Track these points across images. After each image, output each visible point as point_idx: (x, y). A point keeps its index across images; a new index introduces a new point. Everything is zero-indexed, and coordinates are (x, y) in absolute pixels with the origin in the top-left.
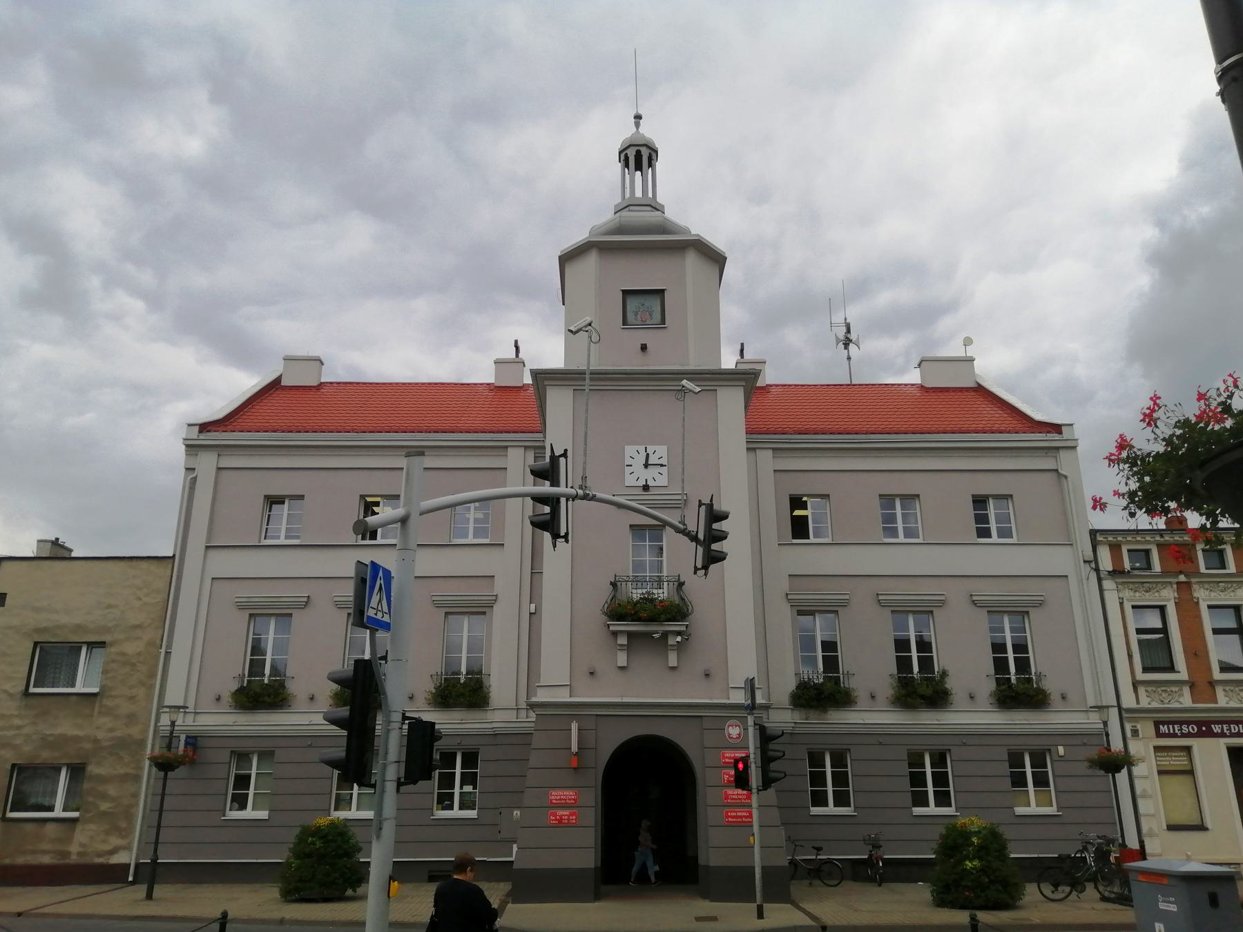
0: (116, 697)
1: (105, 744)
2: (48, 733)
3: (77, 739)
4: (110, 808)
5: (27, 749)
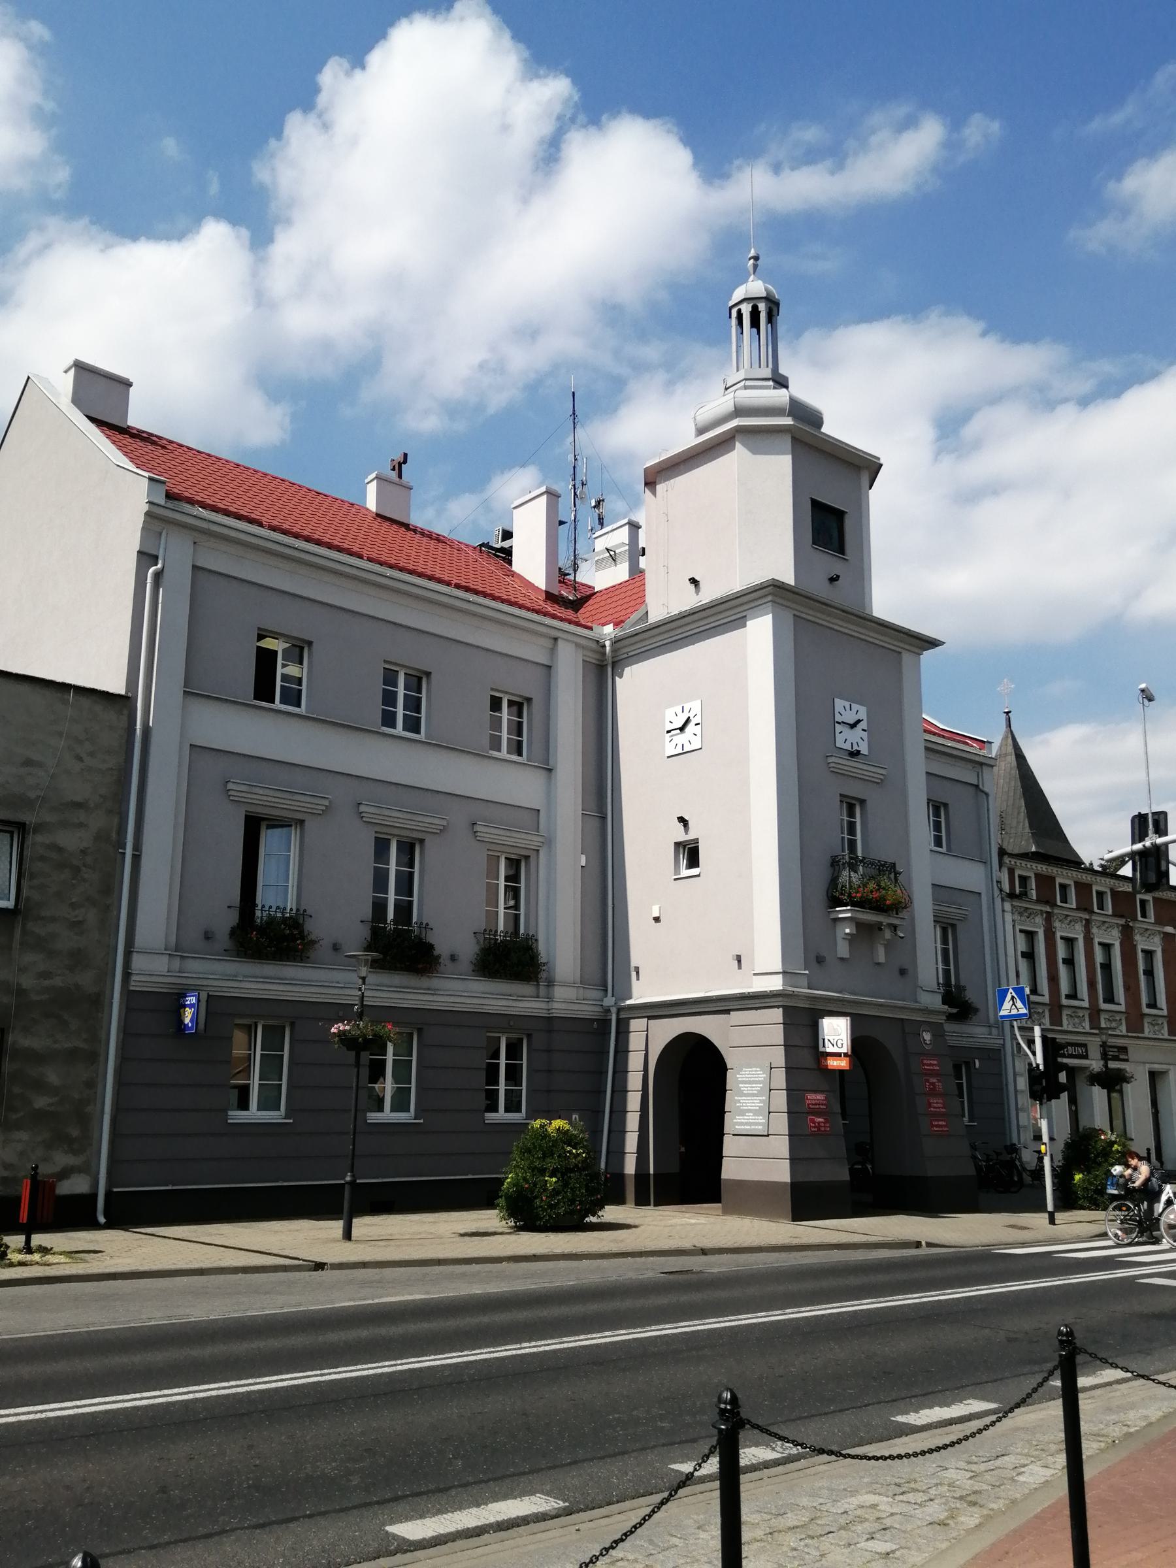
0: (53, 919)
1: (35, 997)
4: (49, 1105)
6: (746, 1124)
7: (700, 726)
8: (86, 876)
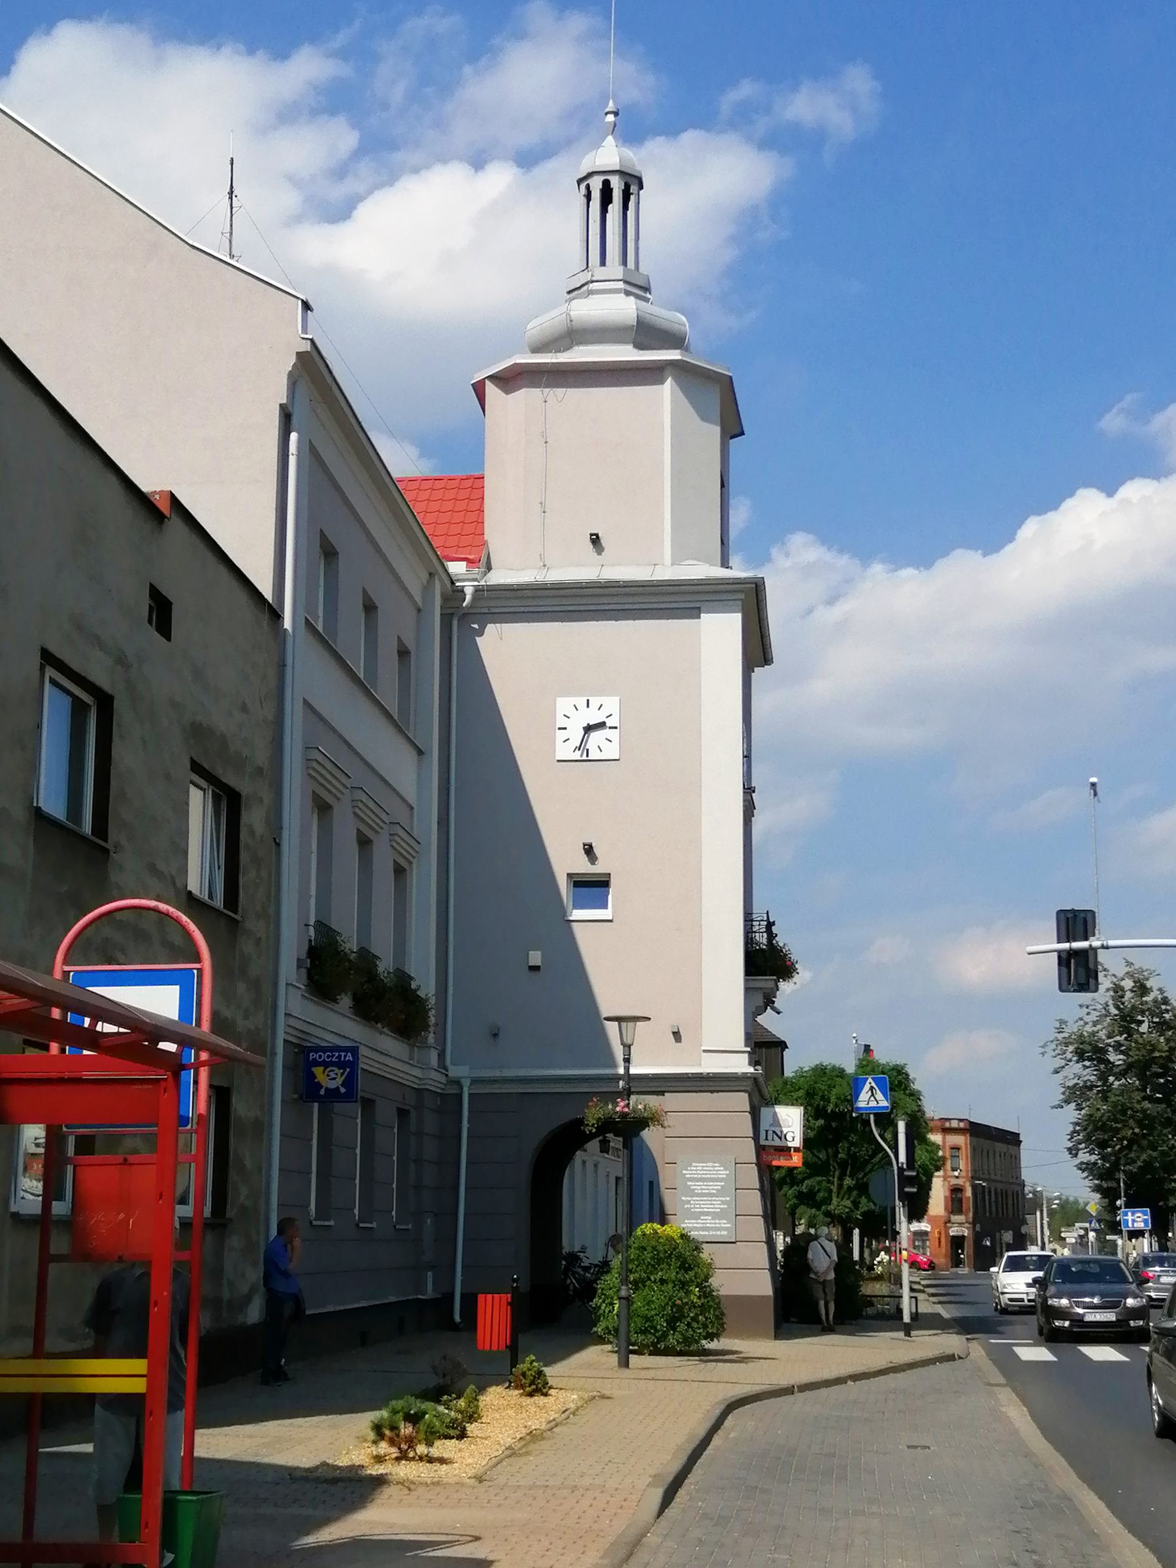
6: (703, 1229)
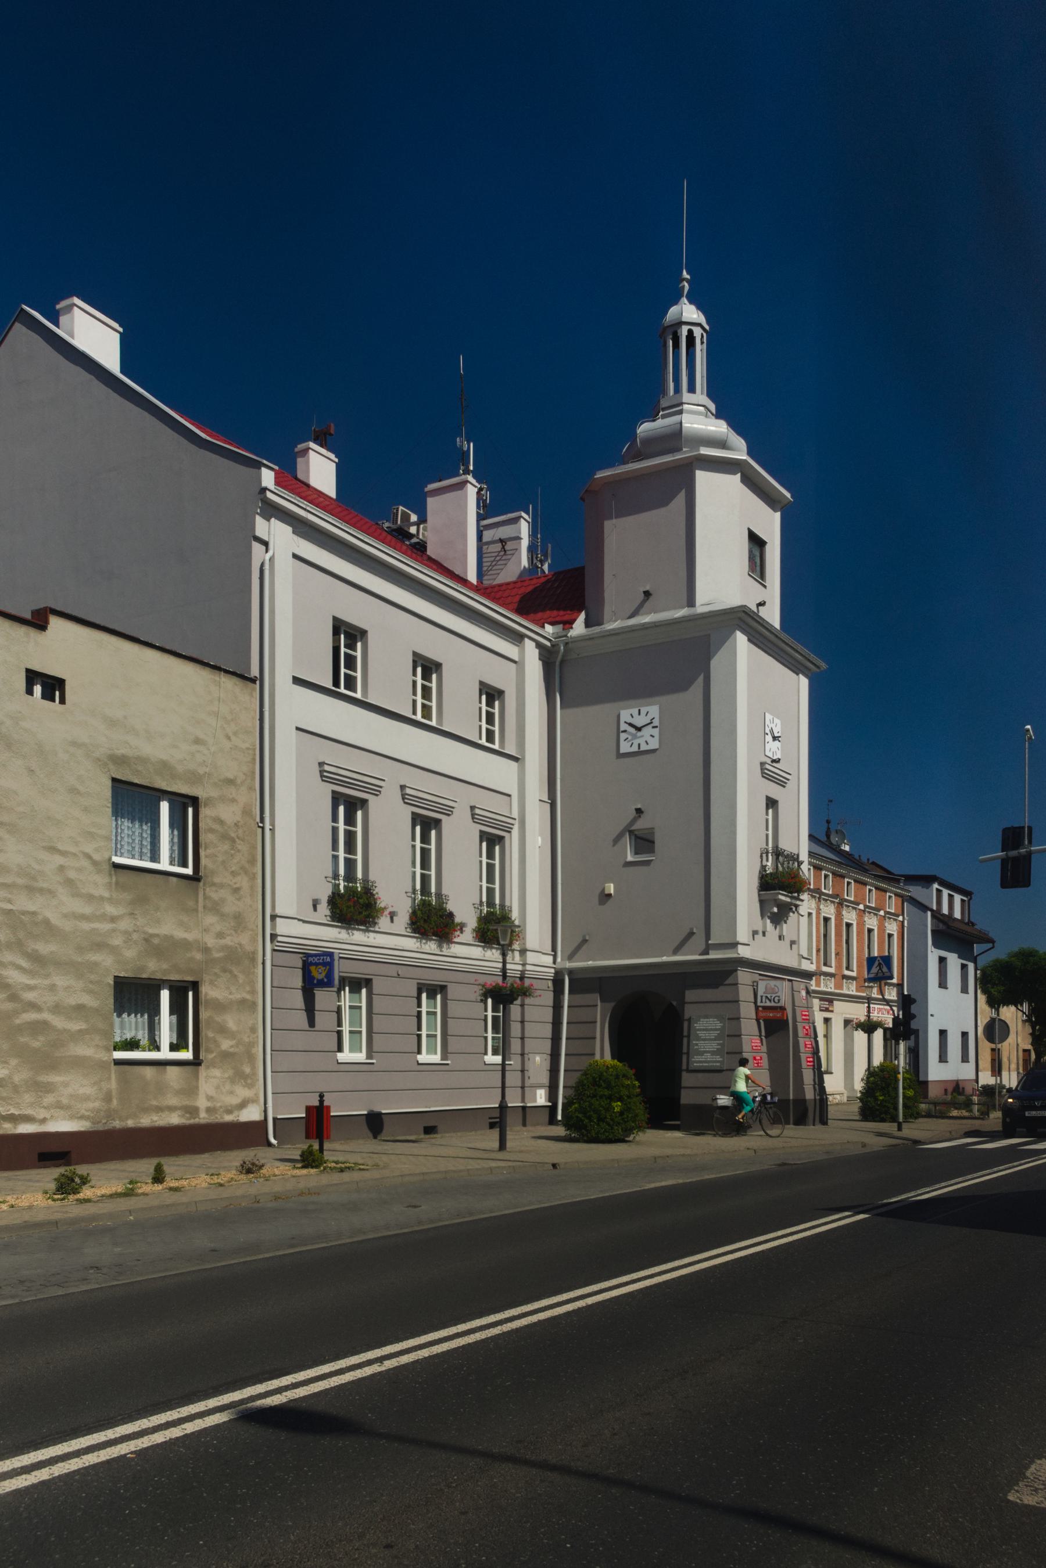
0: (222, 886)
1: (217, 955)
2: (151, 931)
3: (186, 945)
4: (232, 1047)
5: (130, 954)
7: (658, 729)
8: (240, 847)
